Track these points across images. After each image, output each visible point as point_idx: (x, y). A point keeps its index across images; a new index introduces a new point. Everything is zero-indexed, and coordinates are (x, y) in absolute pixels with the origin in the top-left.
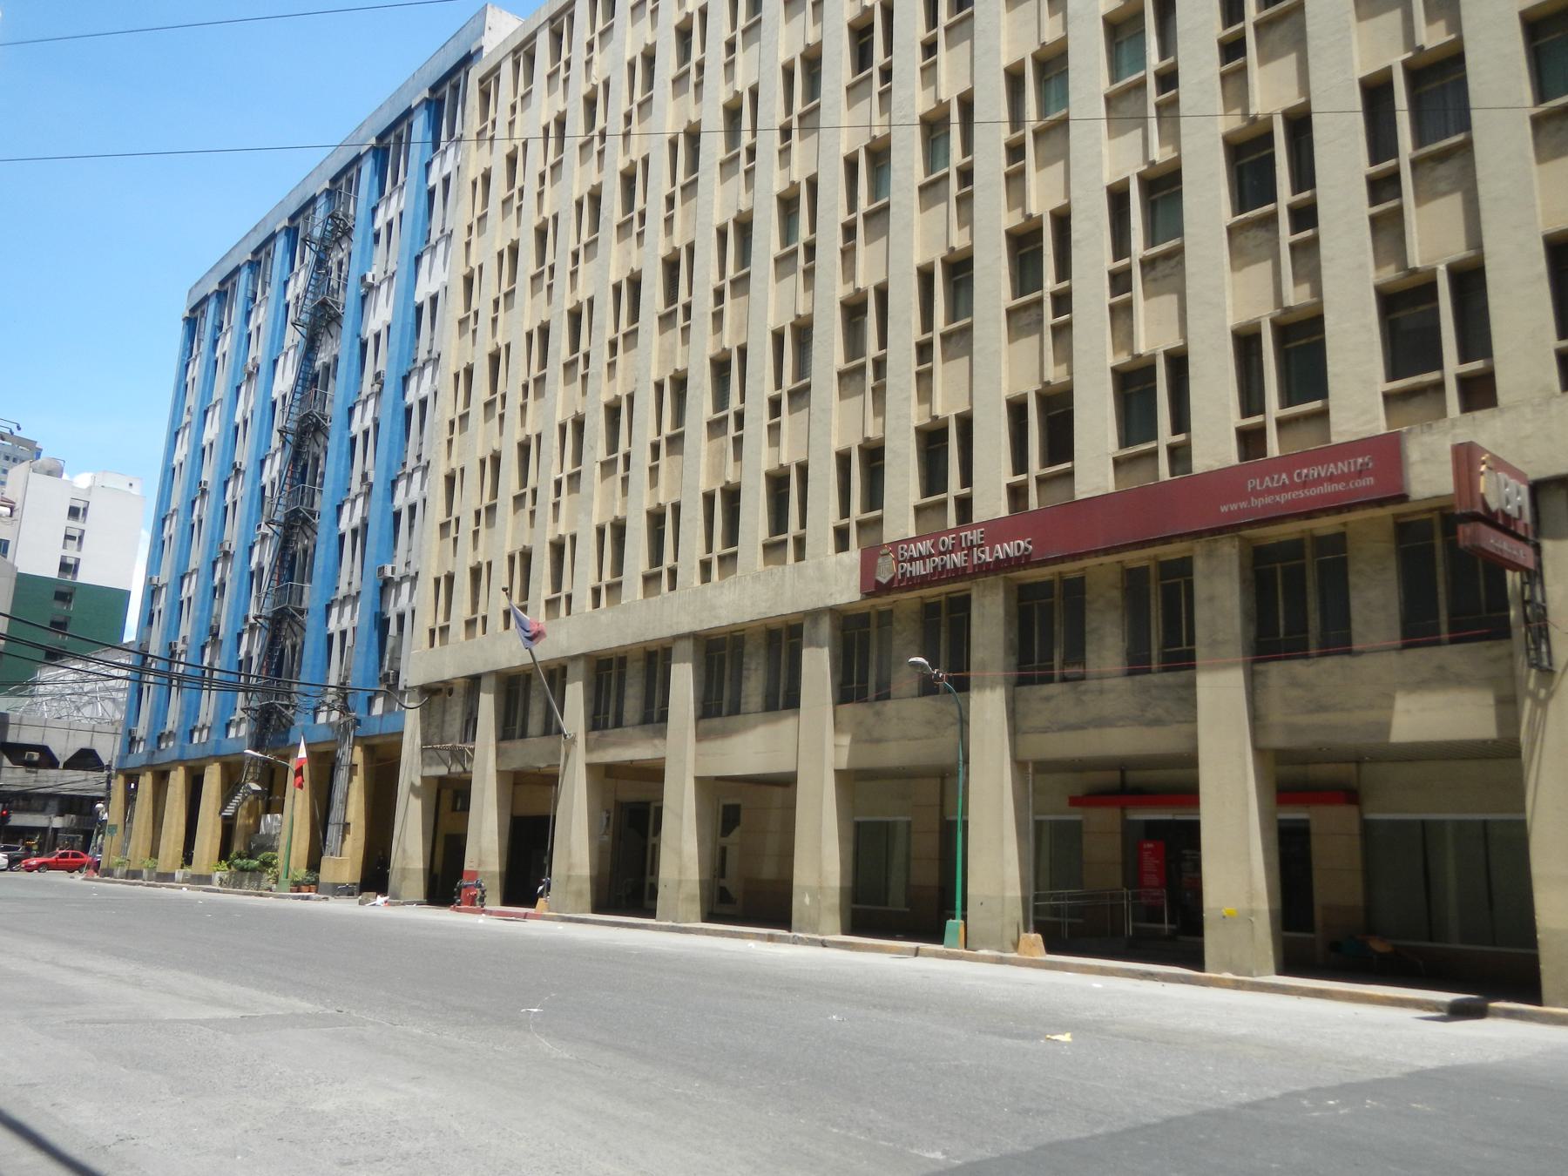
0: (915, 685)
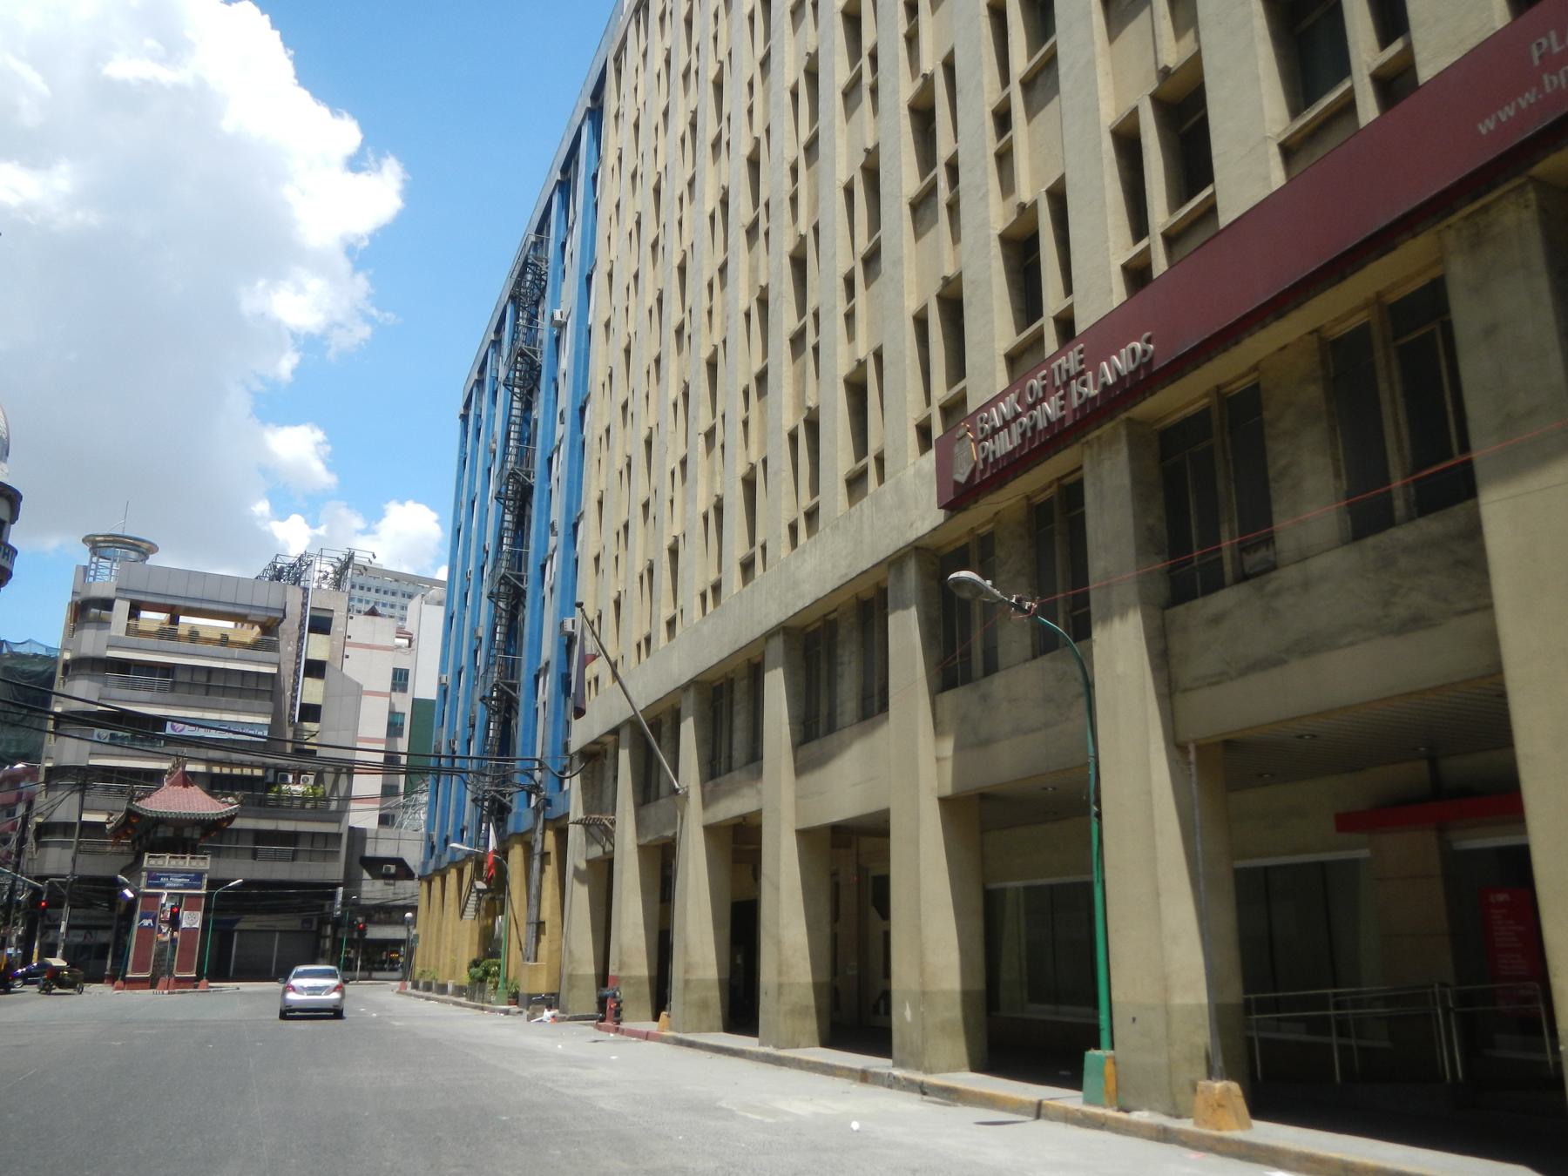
0: (1028, 641)
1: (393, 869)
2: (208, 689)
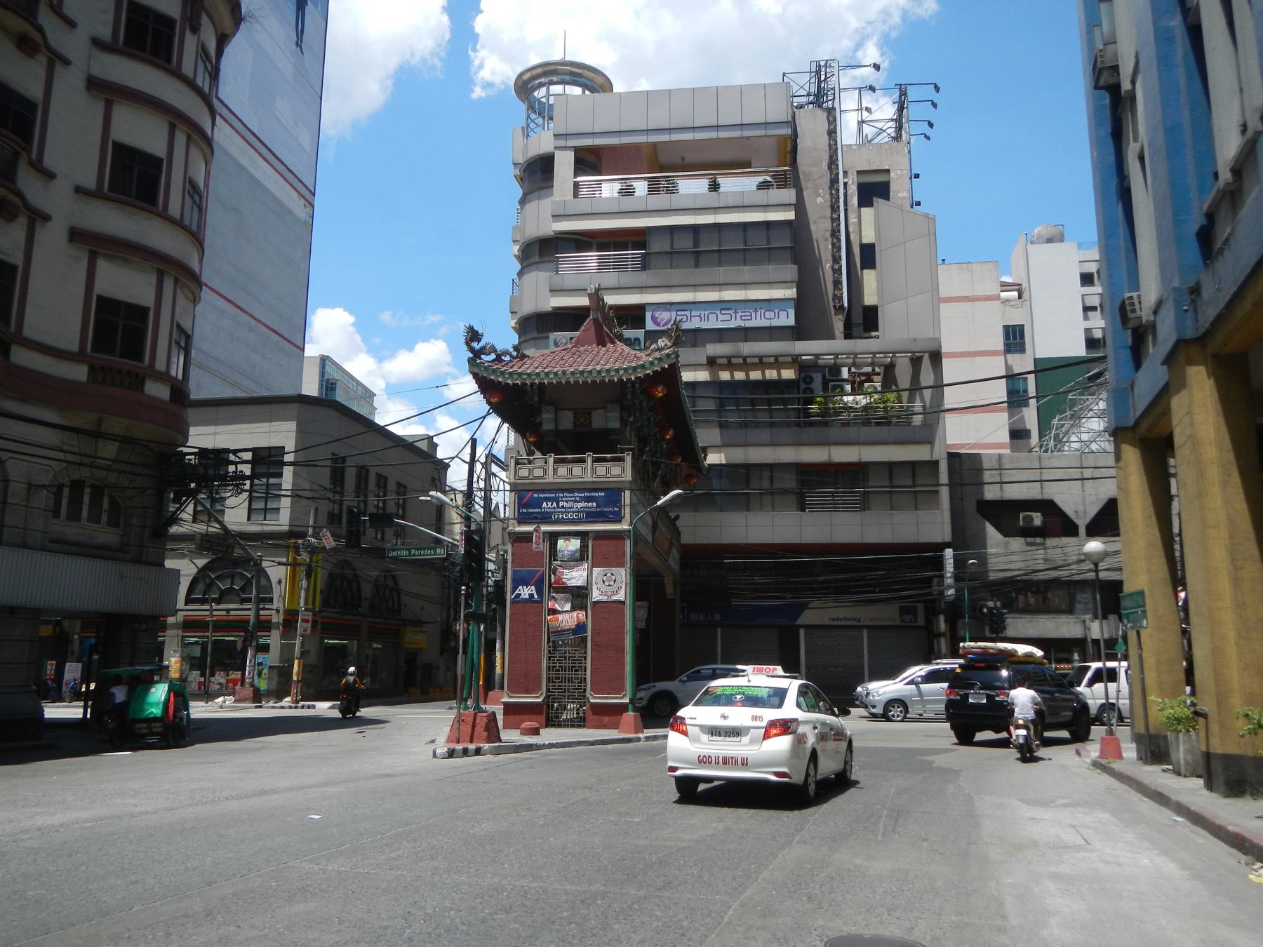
1: (1037, 519)
2: (698, 258)
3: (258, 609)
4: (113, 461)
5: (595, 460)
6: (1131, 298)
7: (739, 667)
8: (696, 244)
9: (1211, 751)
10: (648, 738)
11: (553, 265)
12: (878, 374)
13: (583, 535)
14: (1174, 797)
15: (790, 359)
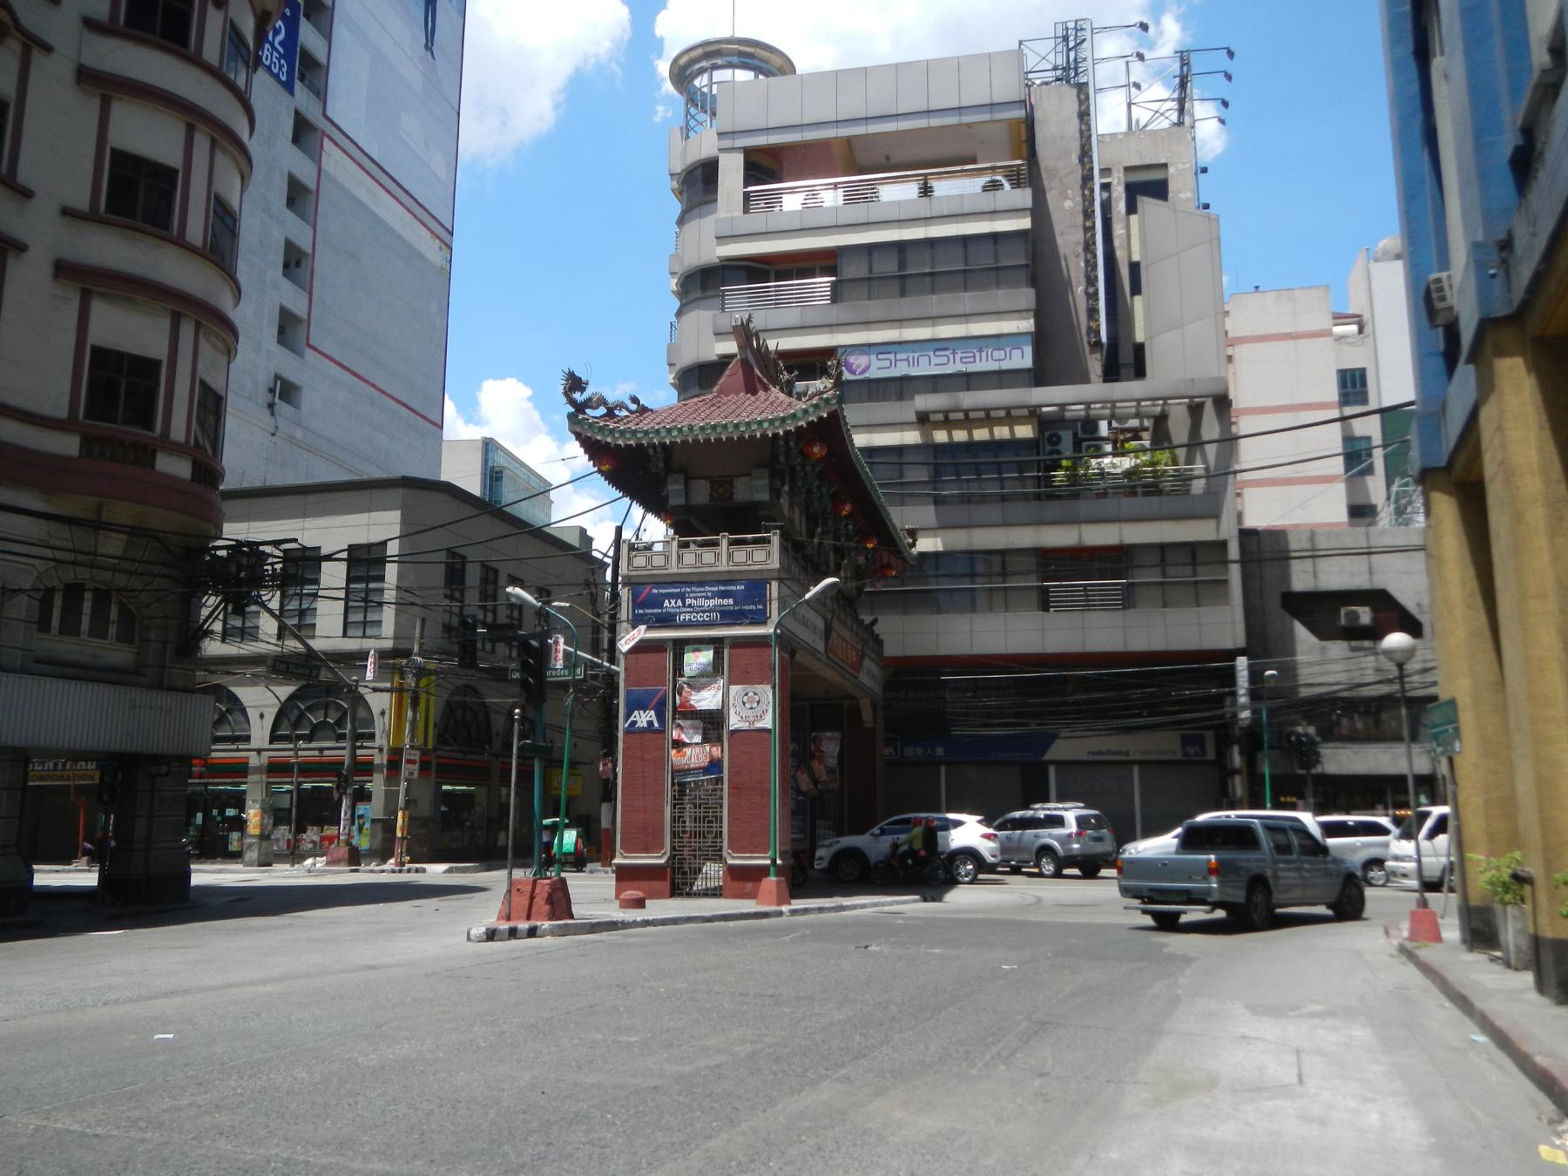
1: (1365, 615)
2: (904, 284)
3: (354, 748)
4: (120, 558)
5: (733, 543)
6: (1439, 280)
7: (951, 816)
8: (902, 266)
9: (1541, 934)
10: (794, 912)
11: (718, 301)
12: (1146, 429)
13: (717, 644)
14: (1480, 1004)
15: (1025, 412)
